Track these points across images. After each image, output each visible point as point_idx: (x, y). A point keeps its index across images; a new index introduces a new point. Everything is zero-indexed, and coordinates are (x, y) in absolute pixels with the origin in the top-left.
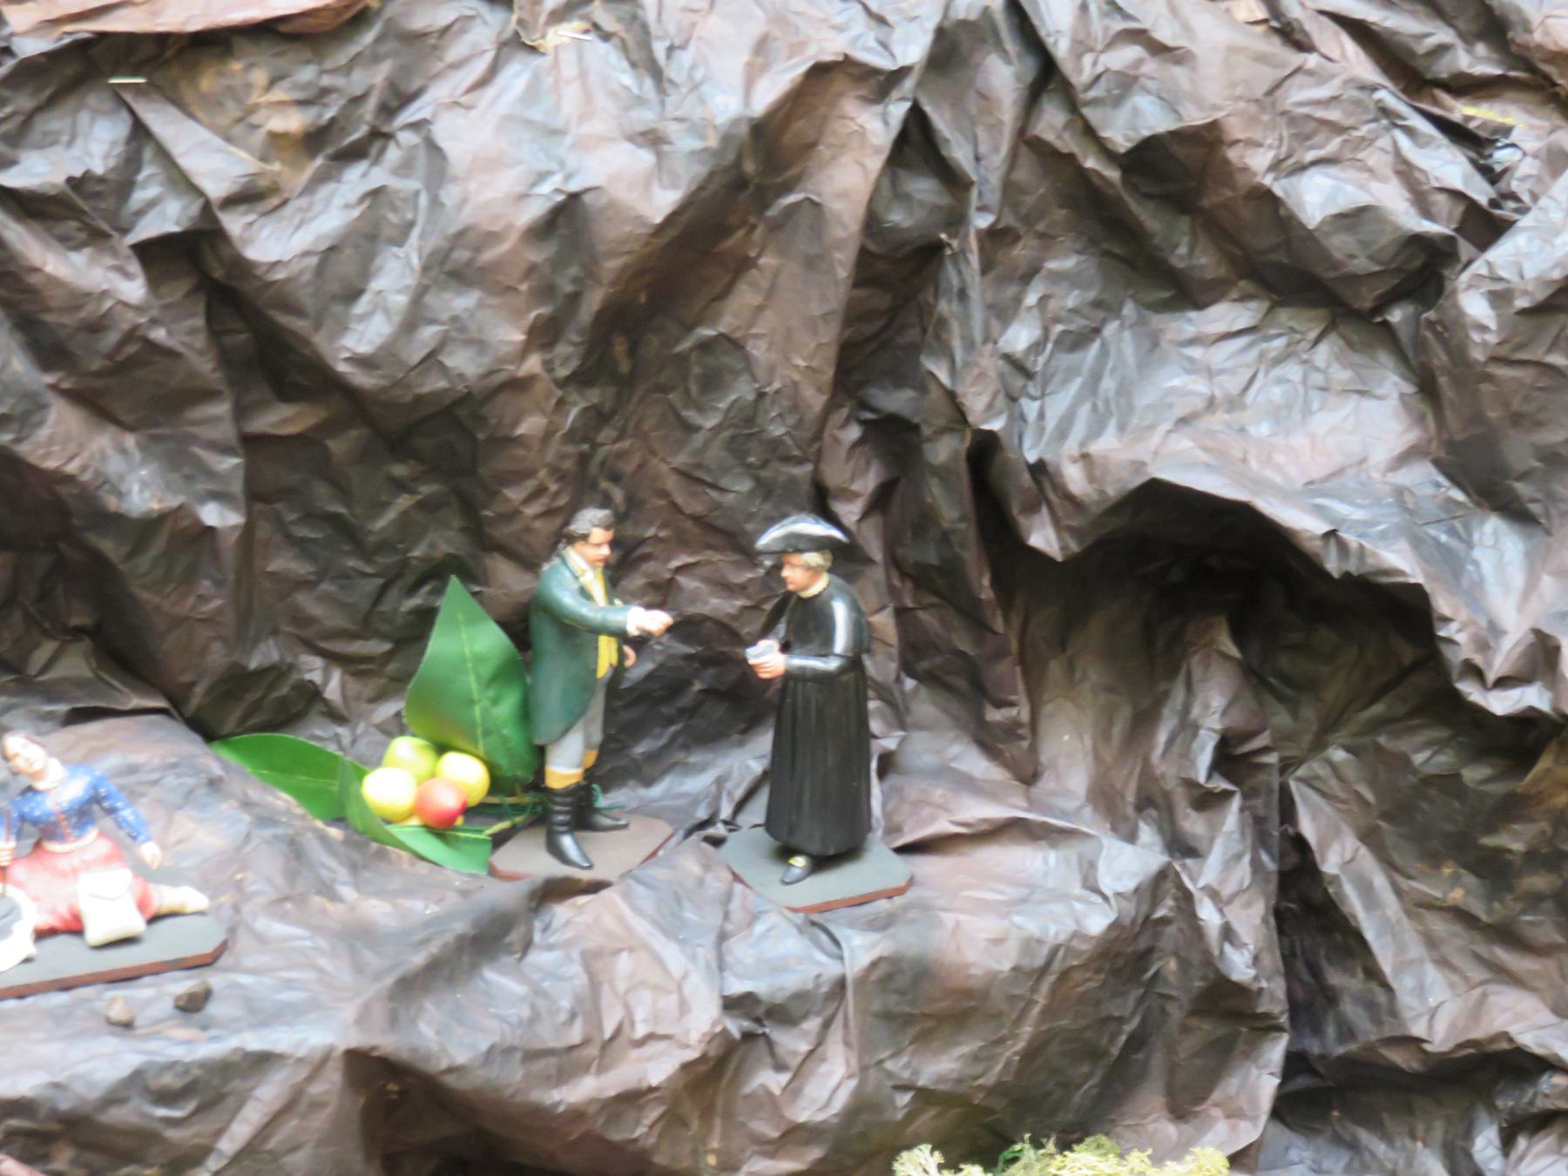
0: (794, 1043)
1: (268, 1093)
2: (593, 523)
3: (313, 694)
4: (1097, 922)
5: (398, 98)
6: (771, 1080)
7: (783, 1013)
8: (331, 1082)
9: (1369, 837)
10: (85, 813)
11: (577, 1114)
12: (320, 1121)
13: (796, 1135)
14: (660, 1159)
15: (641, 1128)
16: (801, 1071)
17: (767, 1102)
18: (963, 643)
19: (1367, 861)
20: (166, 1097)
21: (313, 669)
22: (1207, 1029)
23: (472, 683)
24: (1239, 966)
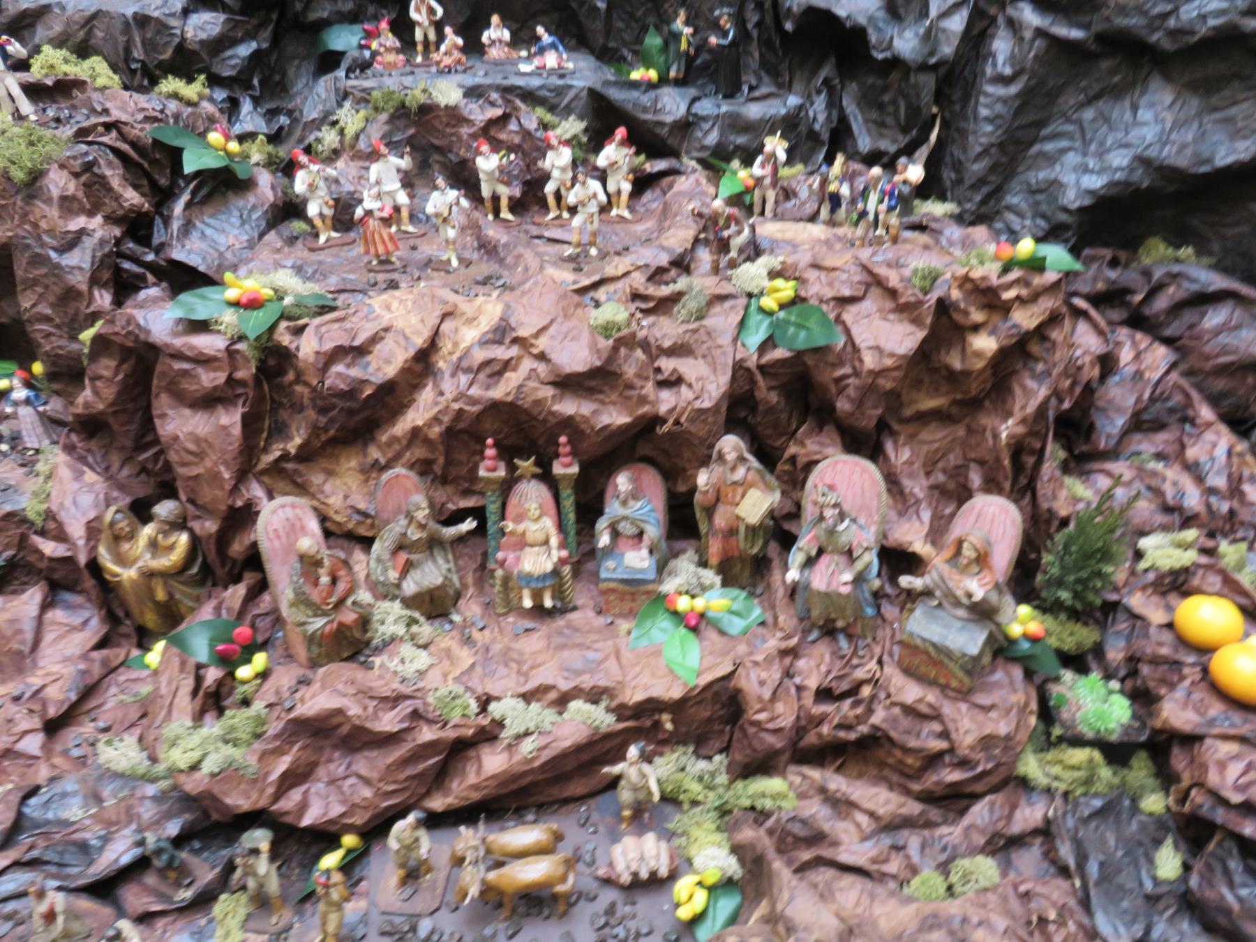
0: (706, 126)
1: (571, 94)
2: (682, 14)
3: (625, 59)
4: (783, 111)
6: (700, 134)
7: (704, 119)
8: (584, 93)
9: (859, 105)
10: (553, 46)
11: (645, 122)
12: (583, 102)
13: (703, 148)
14: (670, 141)
15: (664, 132)
16: (707, 133)
17: (699, 140)
18: (773, 60)
19: (857, 112)
20: (550, 90)
21: (625, 52)
22: (810, 144)
23: (654, 51)
24: (817, 127)
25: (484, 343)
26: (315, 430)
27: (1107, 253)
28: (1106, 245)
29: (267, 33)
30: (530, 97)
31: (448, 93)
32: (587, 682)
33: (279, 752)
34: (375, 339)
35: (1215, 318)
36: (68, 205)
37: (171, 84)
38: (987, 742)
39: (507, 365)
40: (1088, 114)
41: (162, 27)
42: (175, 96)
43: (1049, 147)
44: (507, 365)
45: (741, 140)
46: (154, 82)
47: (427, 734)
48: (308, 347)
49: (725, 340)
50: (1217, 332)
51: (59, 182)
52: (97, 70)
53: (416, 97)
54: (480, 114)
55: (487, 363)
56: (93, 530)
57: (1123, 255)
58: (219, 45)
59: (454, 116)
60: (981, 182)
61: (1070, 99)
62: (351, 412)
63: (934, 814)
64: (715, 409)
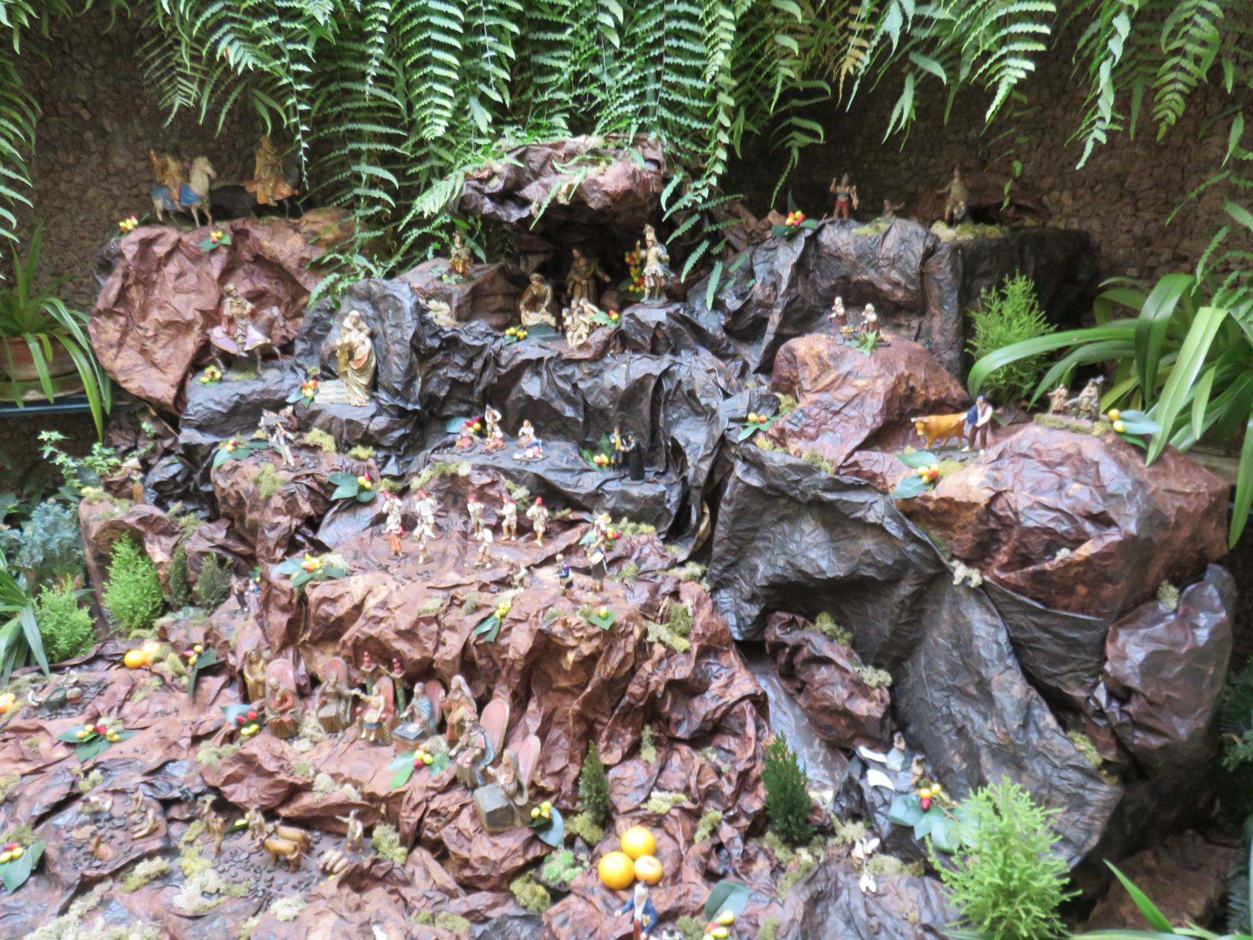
5: (601, 371)
25: (376, 607)
26: (314, 633)
27: (786, 616)
28: (788, 611)
29: (411, 425)
30: (507, 473)
31: (464, 470)
32: (355, 776)
33: (230, 765)
34: (341, 596)
35: (823, 673)
36: (277, 511)
37: (359, 451)
38: (484, 860)
39: (381, 620)
40: (777, 529)
41: (359, 424)
42: (357, 458)
43: (760, 544)
44: (381, 620)
45: (629, 507)
46: (350, 447)
47: (282, 776)
48: (313, 595)
49: (467, 629)
50: (823, 684)
51: (277, 501)
52: (328, 442)
53: (451, 469)
54: (481, 479)
55: (374, 617)
56: (246, 656)
57: (800, 620)
58: (384, 432)
59: (467, 480)
60: (720, 559)
61: (768, 518)
62: (327, 627)
63: (461, 891)
64: (453, 661)
